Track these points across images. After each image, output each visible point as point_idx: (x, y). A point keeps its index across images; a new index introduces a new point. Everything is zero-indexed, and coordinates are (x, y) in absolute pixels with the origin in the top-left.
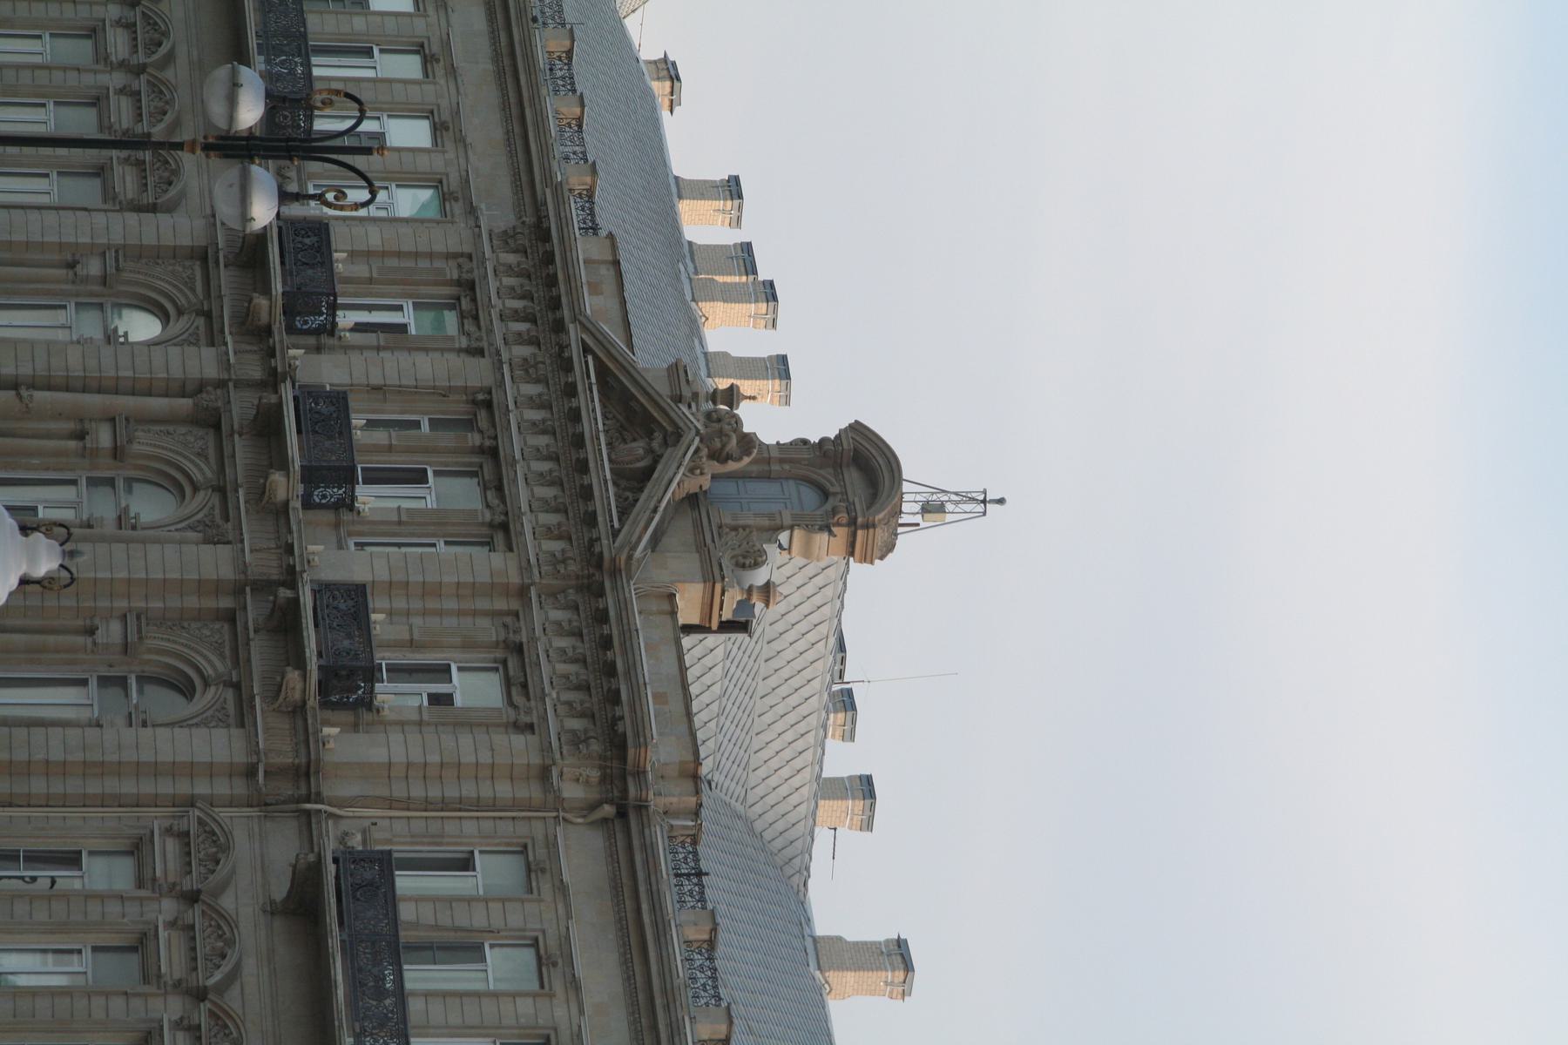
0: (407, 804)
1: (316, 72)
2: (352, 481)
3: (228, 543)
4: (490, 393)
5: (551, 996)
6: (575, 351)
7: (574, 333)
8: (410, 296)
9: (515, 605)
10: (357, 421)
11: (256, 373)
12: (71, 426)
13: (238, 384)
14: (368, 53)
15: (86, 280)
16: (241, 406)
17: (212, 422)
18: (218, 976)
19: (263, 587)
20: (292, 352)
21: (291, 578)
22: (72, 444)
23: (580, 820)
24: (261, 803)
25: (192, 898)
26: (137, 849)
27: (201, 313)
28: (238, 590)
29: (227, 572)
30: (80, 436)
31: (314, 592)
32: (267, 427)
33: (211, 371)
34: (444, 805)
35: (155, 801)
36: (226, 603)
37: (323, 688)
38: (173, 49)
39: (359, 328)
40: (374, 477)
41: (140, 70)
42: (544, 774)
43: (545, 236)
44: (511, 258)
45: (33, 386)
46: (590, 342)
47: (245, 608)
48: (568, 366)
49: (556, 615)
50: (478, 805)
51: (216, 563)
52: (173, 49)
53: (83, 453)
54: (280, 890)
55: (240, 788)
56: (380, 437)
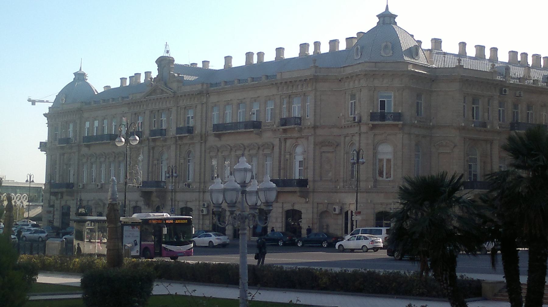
1: (106, 133)
2: (162, 129)
10: (154, 129)
16: (152, 144)
18: (229, 147)
19: (176, 141)
20: (145, 137)
21: (175, 137)
24: (205, 142)
26: (211, 158)
31: (177, 134)
32: (154, 140)
35: (205, 155)
37: (190, 133)
38: (103, 152)
39: (141, 128)
40: (162, 126)
51: (173, 148)
52: (103, 152)
54: (217, 139)
55: (203, 144)
56: (156, 126)
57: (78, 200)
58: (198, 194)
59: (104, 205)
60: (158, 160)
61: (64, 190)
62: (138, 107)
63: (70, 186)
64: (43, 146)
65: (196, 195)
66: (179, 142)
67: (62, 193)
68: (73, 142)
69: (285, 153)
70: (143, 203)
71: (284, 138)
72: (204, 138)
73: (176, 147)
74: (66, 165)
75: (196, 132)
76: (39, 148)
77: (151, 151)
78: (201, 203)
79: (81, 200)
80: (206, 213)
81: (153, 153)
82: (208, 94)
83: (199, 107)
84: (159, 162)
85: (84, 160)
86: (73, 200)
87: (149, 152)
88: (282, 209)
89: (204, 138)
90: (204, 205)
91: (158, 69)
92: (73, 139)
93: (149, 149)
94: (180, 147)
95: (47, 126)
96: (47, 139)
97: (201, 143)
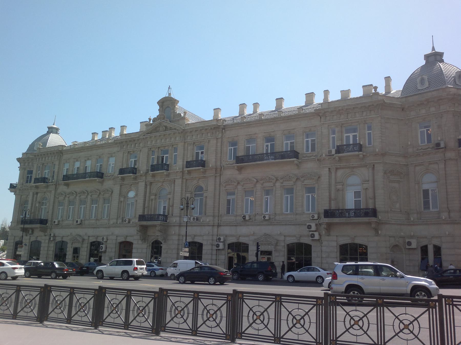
0: (221, 156)
3: (175, 180)
4: (149, 148)
5: (257, 137)
6: (144, 137)
7: (142, 137)
8: (129, 160)
9: (186, 144)
11: (144, 178)
12: (151, 202)
13: (183, 176)
14: (86, 167)
15: (124, 200)
17: (151, 183)
22: (154, 201)
23: (224, 135)
25: (238, 183)
27: (131, 185)
28: (183, 179)
29: (180, 180)
30: (152, 200)
33: (144, 183)
34: (221, 152)
36: (185, 181)
41: (66, 196)
42: (217, 139)
43: (122, 142)
44: (125, 147)
45: (145, 206)
46: (143, 135)
47: (186, 178)
48: (146, 138)
49: (189, 138)
50: (221, 148)
51: (178, 182)
53: (155, 200)
57: (52, 235)
58: (211, 228)
59: (83, 240)
60: (156, 195)
61: (38, 225)
62: (133, 146)
63: (43, 222)
64: (12, 187)
65: (207, 230)
66: (187, 176)
67: (33, 230)
68: (50, 181)
69: (336, 183)
70: (139, 237)
71: (336, 168)
72: (219, 170)
73: (182, 181)
74: (39, 203)
75: (210, 166)
76: (8, 189)
77: (148, 187)
78: (215, 238)
79: (54, 236)
80: (223, 248)
81: (150, 188)
82: (224, 129)
83: (213, 142)
84: (156, 196)
85: (61, 198)
86: (45, 236)
87: (146, 187)
88: (337, 243)
89: (219, 170)
90: (219, 239)
91: (159, 110)
92: (51, 179)
93: (146, 185)
94: (186, 182)
95: (19, 170)
96: (17, 182)
97: (216, 176)
